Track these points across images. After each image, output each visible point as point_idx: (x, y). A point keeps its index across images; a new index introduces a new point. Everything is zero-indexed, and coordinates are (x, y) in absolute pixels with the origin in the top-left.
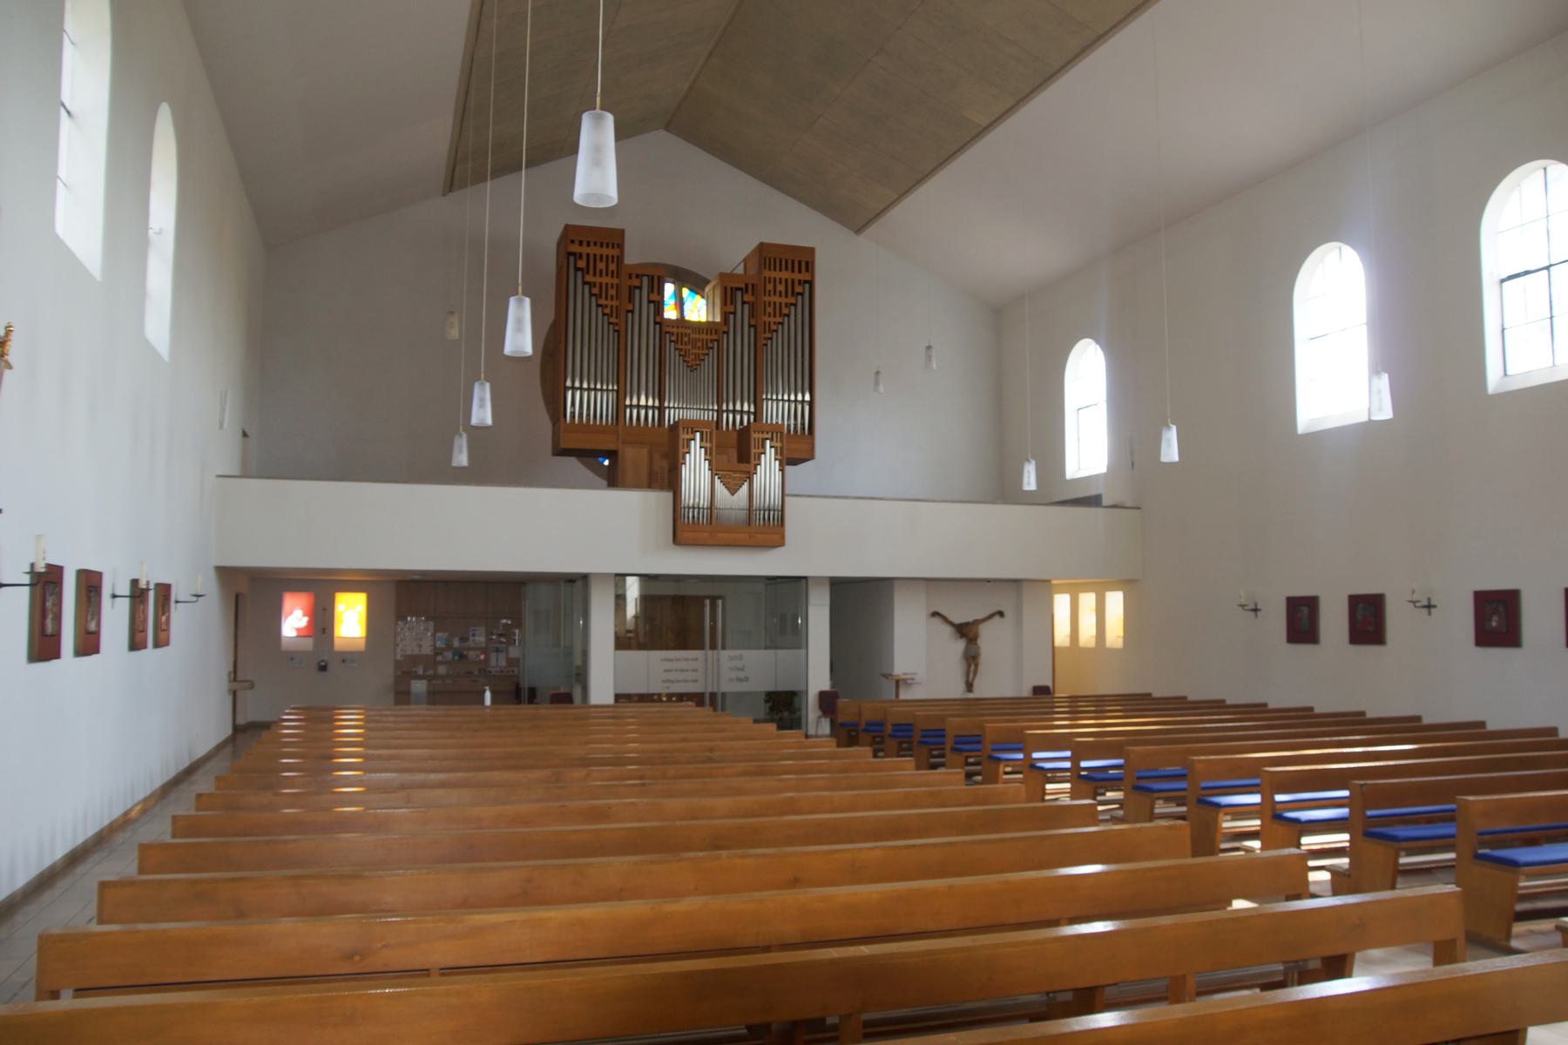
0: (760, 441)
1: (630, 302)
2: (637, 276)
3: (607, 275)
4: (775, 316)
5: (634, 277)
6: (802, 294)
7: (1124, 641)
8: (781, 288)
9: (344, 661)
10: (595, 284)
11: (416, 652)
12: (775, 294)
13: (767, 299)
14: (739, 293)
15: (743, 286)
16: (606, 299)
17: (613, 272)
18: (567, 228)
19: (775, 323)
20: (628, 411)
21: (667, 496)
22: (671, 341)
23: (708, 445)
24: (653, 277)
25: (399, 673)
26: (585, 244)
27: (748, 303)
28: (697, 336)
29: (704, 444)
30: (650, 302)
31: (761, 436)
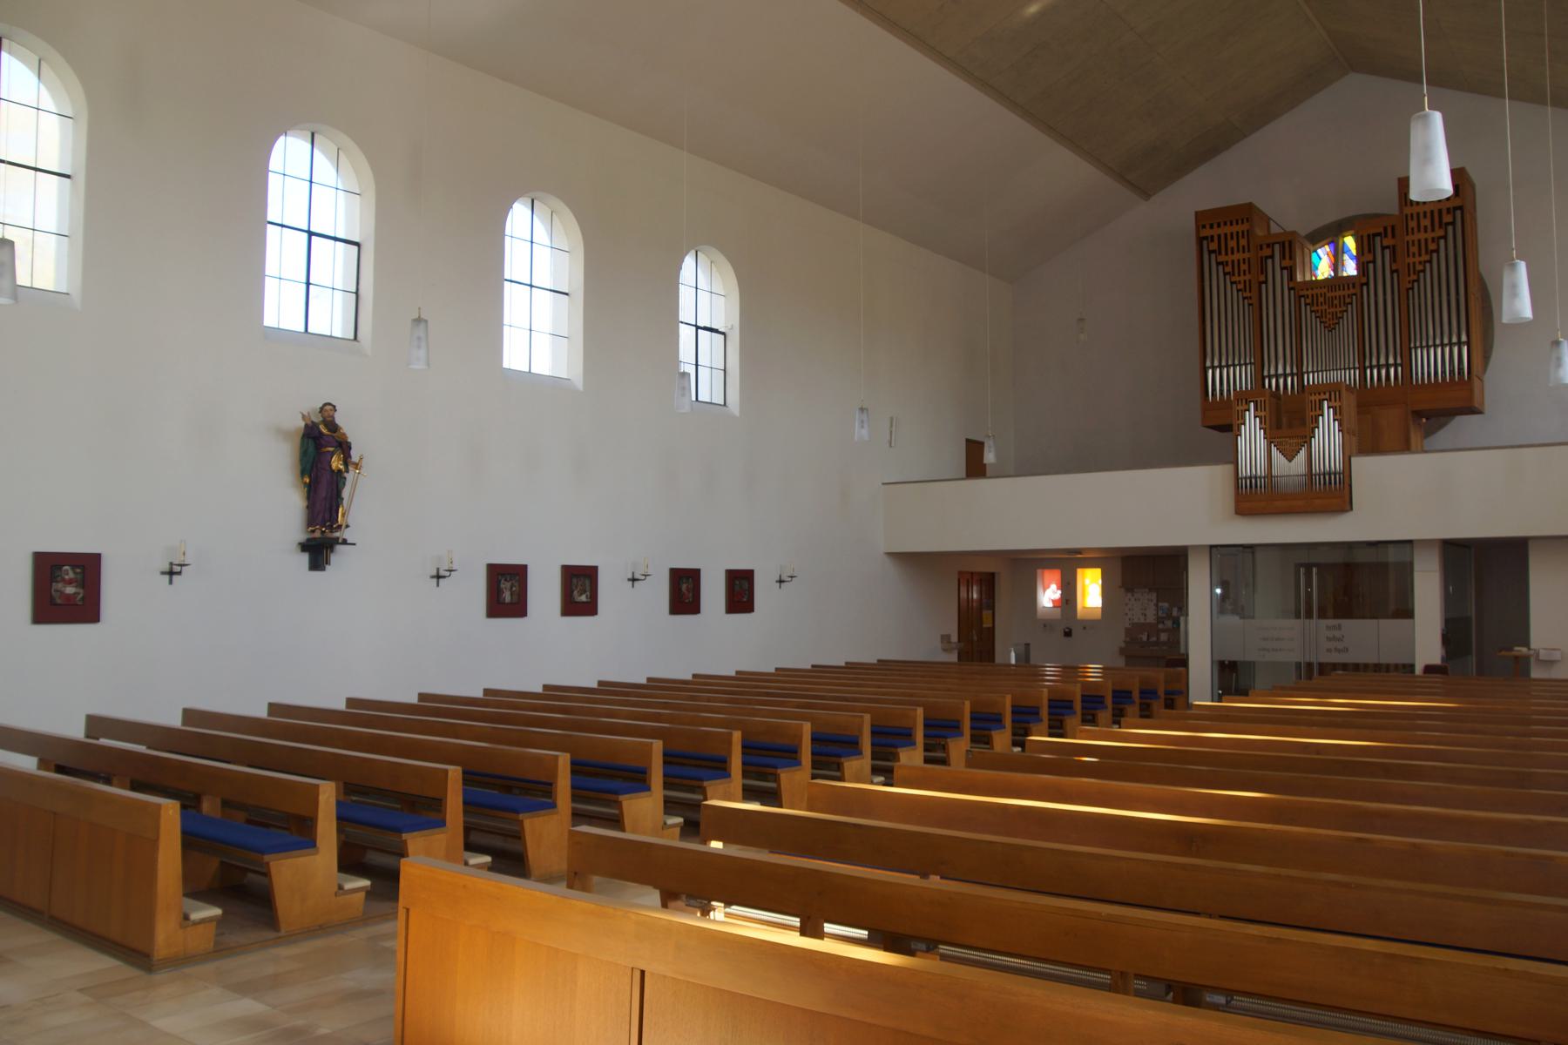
0: (1317, 403)
1: (1262, 273)
2: (1268, 246)
3: (1238, 251)
4: (1420, 255)
5: (1265, 247)
6: (1453, 223)
7: (1102, 611)
8: (1426, 222)
9: (1085, 628)
10: (1227, 262)
11: (1142, 621)
12: (1419, 231)
13: (1409, 238)
14: (1378, 239)
15: (1381, 230)
16: (1239, 275)
17: (1243, 247)
18: (1199, 215)
19: (1420, 263)
20: (1267, 381)
21: (1230, 467)
22: (1306, 305)
23: (1263, 414)
24: (1284, 243)
25: (1128, 639)
26: (1215, 226)
27: (1388, 247)
28: (1333, 294)
29: (1259, 414)
30: (1282, 269)
31: (1317, 397)
